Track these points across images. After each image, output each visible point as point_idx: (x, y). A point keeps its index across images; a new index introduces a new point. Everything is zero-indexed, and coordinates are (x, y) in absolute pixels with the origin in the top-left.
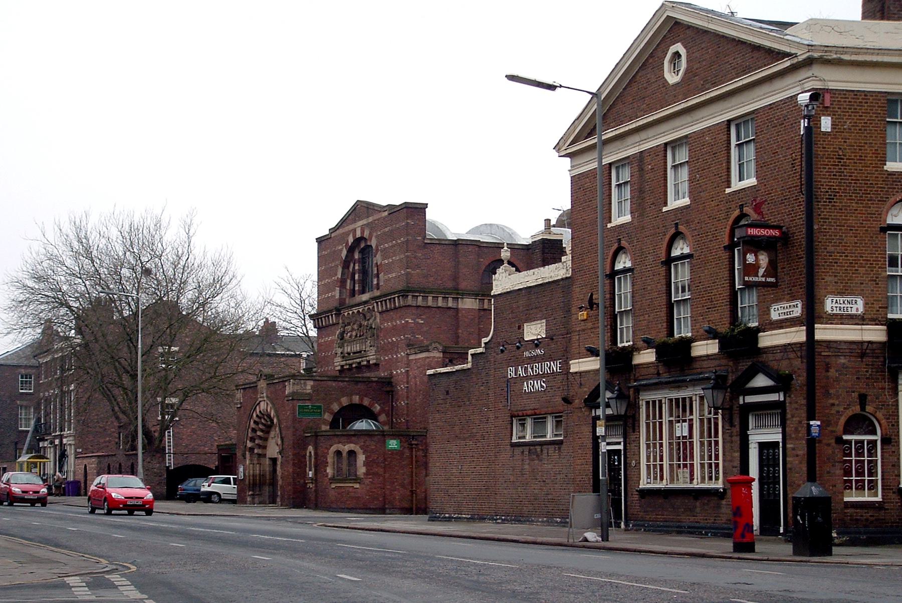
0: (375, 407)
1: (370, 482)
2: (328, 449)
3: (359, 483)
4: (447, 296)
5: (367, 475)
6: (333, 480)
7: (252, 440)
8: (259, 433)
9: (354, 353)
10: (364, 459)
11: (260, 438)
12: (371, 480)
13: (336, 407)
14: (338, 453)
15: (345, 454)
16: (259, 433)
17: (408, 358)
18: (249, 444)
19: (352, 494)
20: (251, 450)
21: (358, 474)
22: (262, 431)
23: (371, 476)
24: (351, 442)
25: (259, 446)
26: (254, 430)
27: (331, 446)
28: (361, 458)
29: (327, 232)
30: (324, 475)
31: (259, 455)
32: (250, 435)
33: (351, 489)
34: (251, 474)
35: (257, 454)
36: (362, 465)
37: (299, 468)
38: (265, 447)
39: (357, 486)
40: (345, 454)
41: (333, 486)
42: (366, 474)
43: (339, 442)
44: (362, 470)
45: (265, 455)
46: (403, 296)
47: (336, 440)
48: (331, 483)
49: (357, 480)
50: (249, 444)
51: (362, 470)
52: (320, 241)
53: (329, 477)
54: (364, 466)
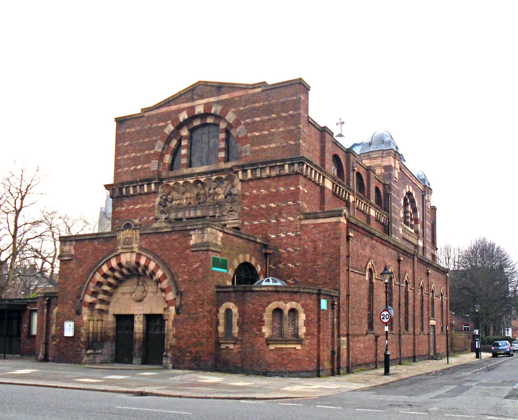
0: (258, 267)
1: (309, 342)
2: (264, 307)
3: (301, 344)
4: (321, 173)
5: (307, 335)
6: (268, 342)
7: (94, 294)
8: (106, 288)
9: (187, 219)
10: (305, 318)
11: (105, 292)
12: (309, 340)
13: (236, 264)
14: (278, 311)
15: (286, 312)
16: (106, 288)
17: (300, 222)
18: (89, 299)
19: (294, 357)
20: (91, 305)
21: (299, 334)
22: (110, 285)
23: (309, 337)
24: (294, 300)
25: (102, 301)
26: (99, 284)
27: (269, 303)
28: (302, 317)
29: (140, 112)
30: (257, 335)
31: (101, 311)
32: (92, 289)
33: (292, 351)
34: (91, 329)
35: (99, 310)
36: (303, 325)
37: (211, 327)
38: (108, 303)
39: (299, 347)
40: (286, 312)
41: (272, 347)
42: (307, 334)
43: (279, 300)
44: (303, 330)
45: (107, 312)
46: (298, 163)
47: (276, 296)
48: (268, 344)
49: (299, 341)
50: (89, 299)
51: (303, 330)
52: (120, 121)
53: (266, 336)
54: (305, 326)
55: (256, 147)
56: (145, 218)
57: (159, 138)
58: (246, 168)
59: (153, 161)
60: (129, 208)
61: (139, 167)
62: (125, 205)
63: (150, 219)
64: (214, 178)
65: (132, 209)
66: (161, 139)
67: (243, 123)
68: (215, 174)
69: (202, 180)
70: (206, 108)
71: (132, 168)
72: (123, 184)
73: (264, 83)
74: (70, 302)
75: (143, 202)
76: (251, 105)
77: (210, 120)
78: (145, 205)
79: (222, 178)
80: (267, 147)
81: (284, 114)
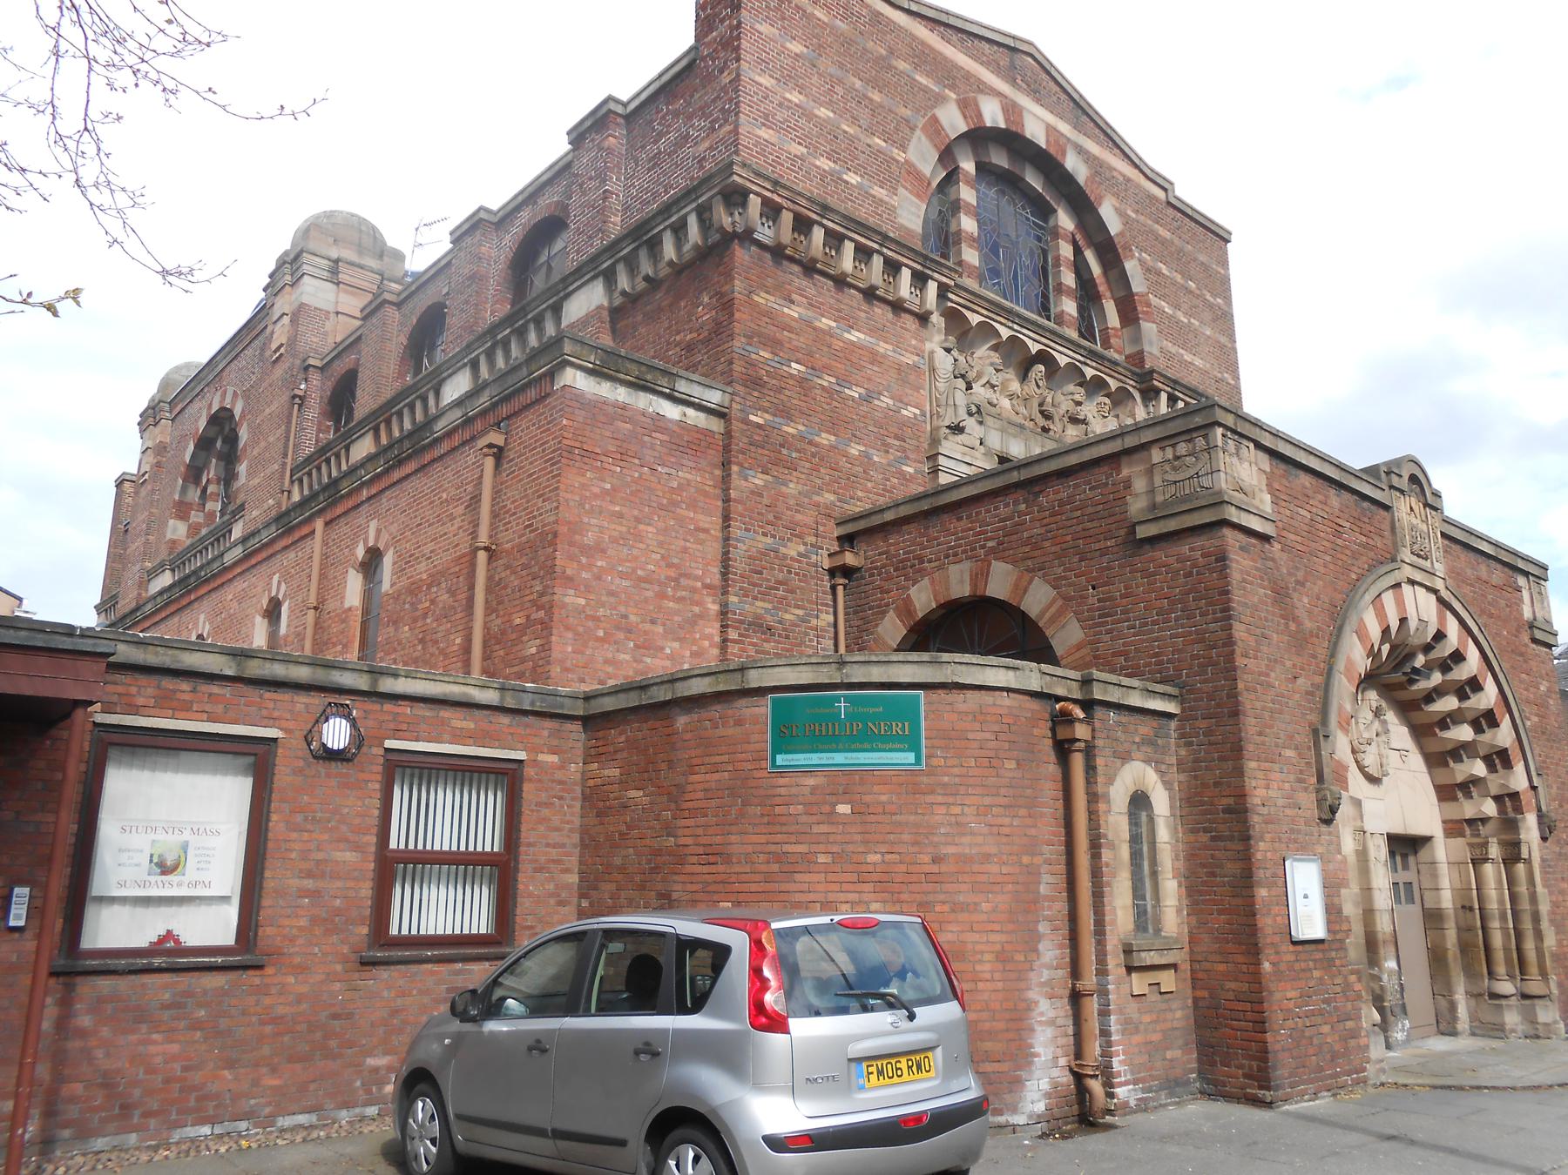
55: (1170, 344)
56: (886, 401)
57: (920, 126)
58: (1177, 393)
59: (901, 190)
60: (817, 324)
61: (853, 179)
62: (794, 296)
63: (904, 412)
64: (1089, 372)
65: (829, 333)
66: (924, 129)
67: (1137, 254)
68: (1094, 364)
69: (1063, 361)
70: (1051, 139)
71: (825, 164)
72: (825, 209)
73: (1165, 185)
74: (1289, 753)
75: (876, 331)
76: (1150, 222)
77: (1034, 180)
78: (883, 348)
79: (1106, 384)
80: (1189, 360)
81: (1208, 297)
